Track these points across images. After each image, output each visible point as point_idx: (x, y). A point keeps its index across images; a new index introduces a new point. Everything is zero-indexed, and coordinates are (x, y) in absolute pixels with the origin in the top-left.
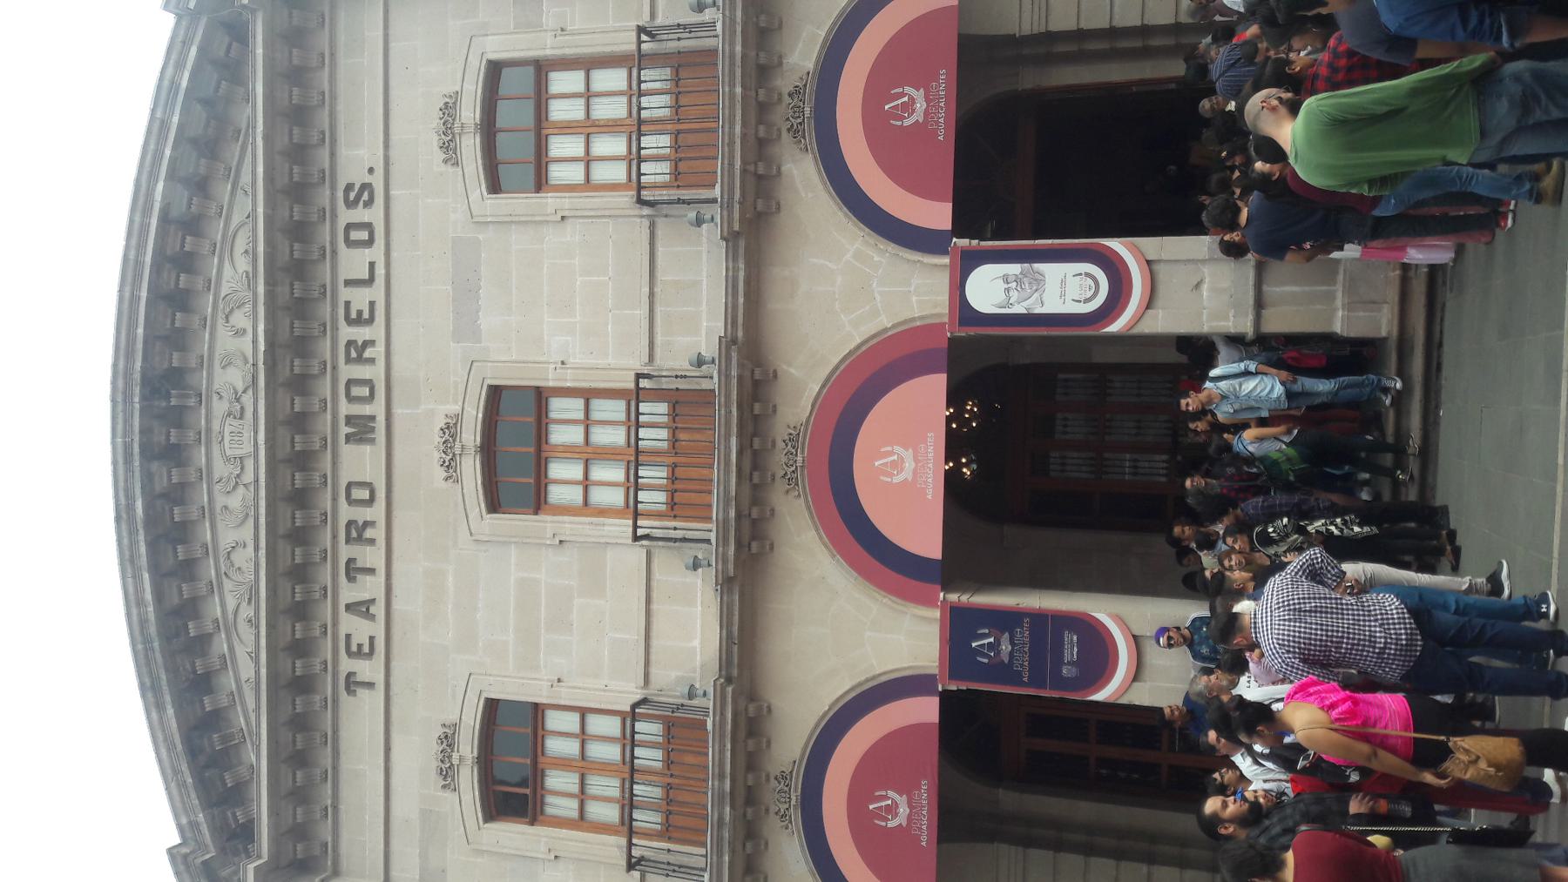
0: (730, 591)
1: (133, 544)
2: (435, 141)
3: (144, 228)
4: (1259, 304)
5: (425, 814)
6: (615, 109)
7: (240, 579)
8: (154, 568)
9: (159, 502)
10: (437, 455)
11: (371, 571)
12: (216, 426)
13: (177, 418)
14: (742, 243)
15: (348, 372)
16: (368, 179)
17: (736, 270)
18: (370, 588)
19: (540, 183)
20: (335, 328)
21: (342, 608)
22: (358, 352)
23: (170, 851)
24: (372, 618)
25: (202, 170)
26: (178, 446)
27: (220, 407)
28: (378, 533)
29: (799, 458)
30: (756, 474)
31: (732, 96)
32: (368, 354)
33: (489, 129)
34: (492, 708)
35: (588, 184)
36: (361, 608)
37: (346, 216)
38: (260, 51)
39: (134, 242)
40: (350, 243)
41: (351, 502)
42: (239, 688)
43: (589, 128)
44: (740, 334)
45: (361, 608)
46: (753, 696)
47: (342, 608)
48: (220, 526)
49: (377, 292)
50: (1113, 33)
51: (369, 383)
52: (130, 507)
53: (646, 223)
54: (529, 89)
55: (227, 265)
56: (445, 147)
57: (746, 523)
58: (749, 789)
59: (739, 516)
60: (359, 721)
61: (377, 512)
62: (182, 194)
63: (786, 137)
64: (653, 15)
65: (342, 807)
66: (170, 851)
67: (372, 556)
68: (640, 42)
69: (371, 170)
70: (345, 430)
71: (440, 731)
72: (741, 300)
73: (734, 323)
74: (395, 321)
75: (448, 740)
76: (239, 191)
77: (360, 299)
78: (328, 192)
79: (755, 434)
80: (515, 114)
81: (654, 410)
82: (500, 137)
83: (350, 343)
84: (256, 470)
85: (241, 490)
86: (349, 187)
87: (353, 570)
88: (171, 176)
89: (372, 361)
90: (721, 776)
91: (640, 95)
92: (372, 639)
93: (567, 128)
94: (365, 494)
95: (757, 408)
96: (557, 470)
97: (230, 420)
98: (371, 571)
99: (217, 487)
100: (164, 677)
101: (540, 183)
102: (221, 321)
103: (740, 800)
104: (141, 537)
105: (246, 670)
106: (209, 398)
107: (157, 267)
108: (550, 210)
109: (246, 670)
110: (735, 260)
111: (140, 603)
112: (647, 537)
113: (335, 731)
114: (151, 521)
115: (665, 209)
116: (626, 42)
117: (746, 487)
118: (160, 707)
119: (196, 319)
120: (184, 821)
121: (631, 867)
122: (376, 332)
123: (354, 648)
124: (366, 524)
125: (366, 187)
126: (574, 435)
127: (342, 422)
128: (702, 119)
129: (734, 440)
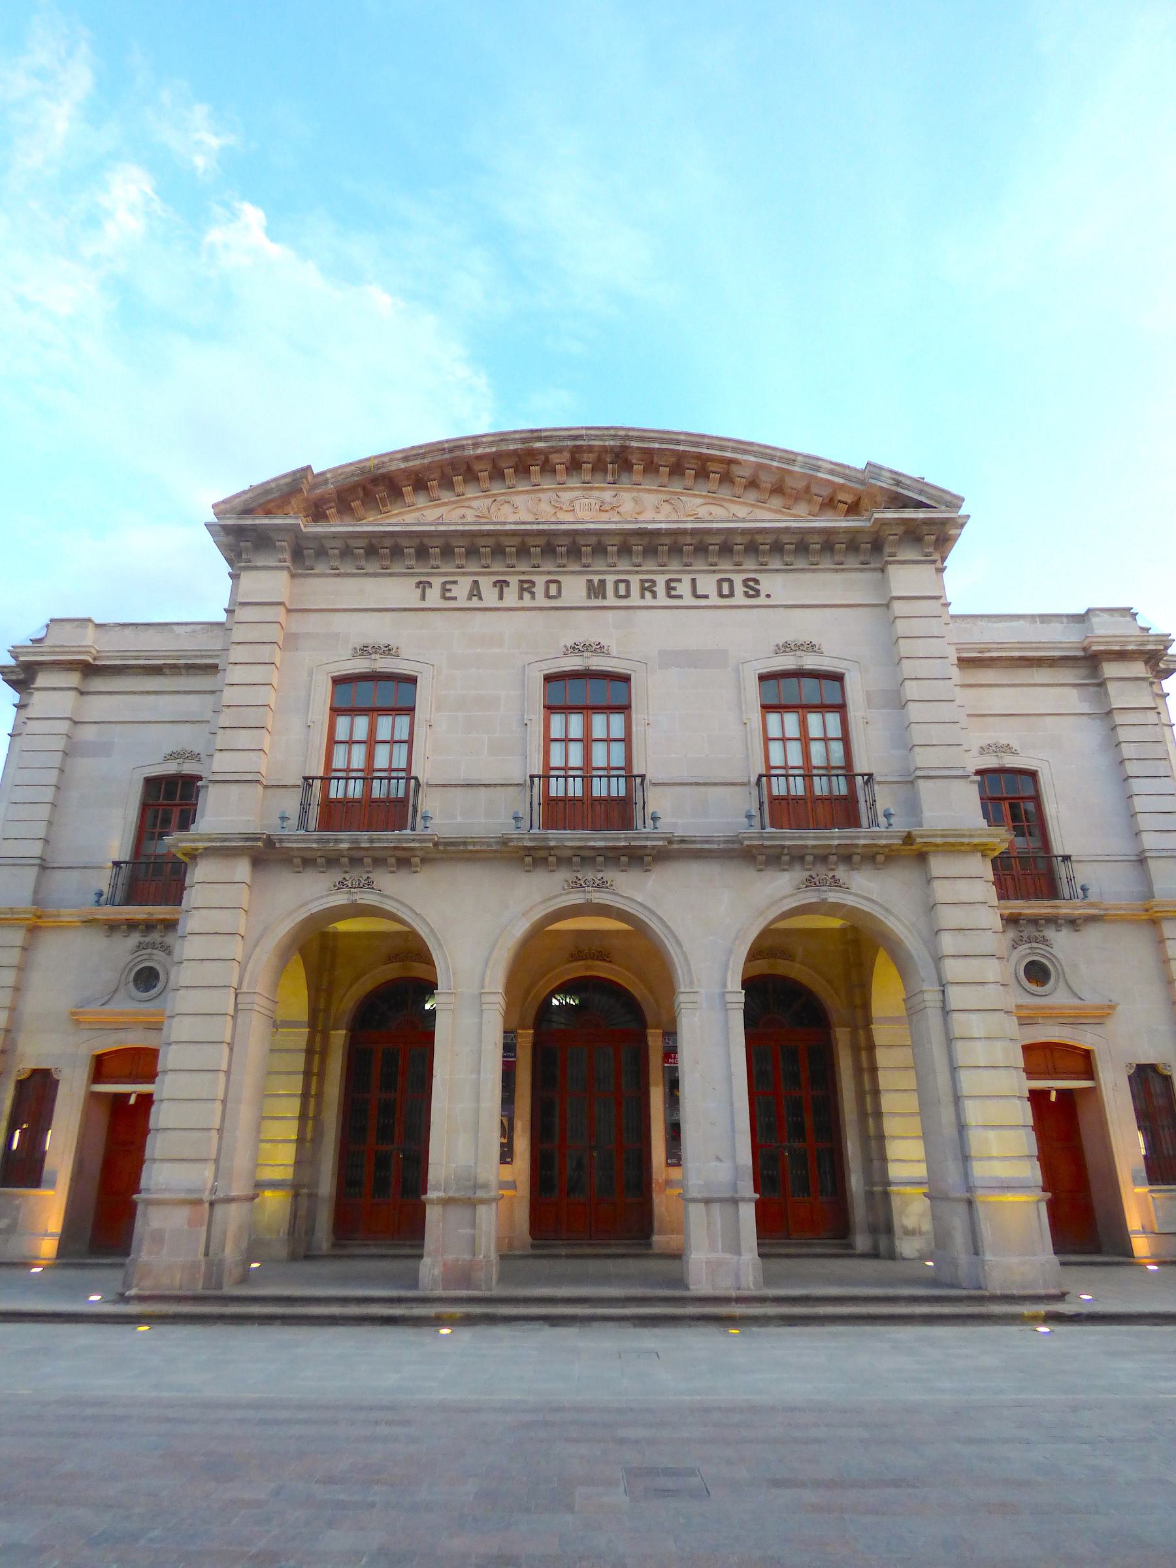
0: (498, 843)
1: (515, 441)
2: (790, 639)
3: (725, 448)
4: (708, 1201)
6: (817, 759)
7: (493, 509)
8: (498, 455)
9: (543, 457)
10: (581, 640)
11: (501, 598)
12: (596, 493)
13: (599, 467)
14: (736, 846)
15: (635, 580)
16: (763, 594)
18: (490, 596)
19: (767, 708)
20: (663, 572)
21: (475, 578)
22: (648, 588)
23: (309, 468)
24: (469, 599)
25: (763, 485)
26: (580, 468)
27: (607, 496)
29: (590, 889)
30: (578, 859)
32: (648, 594)
33: (799, 674)
34: (412, 680)
35: (767, 740)
36: (475, 591)
37: (738, 580)
38: (844, 524)
40: (720, 582)
42: (418, 509)
43: (805, 740)
44: (675, 846)
45: (475, 591)
46: (424, 860)
47: (475, 578)
49: (689, 600)
50: (876, 1092)
52: (540, 439)
53: (746, 780)
54: (827, 702)
55: (699, 501)
56: (786, 645)
57: (543, 854)
60: (396, 590)
61: (540, 600)
62: (746, 472)
64: (879, 783)
65: (338, 579)
66: (309, 468)
68: (863, 775)
69: (768, 596)
70: (596, 579)
71: (393, 645)
72: (699, 846)
73: (683, 841)
74: (668, 611)
75: (388, 651)
76: (750, 509)
77: (684, 588)
78: (753, 568)
79: (605, 858)
80: (809, 690)
81: (618, 788)
82: (795, 680)
83: (653, 582)
84: (567, 520)
86: (756, 581)
87: (501, 585)
88: (760, 466)
89: (643, 597)
90: (371, 840)
92: (455, 598)
95: (624, 859)
97: (599, 503)
98: (501, 598)
99: (552, 495)
100: (426, 461)
101: (767, 708)
102: (664, 497)
104: (519, 446)
105: (431, 514)
107: (699, 457)
109: (431, 514)
112: (532, 782)
113: (391, 575)
114: (531, 453)
115: (755, 792)
117: (570, 853)
118: (406, 459)
120: (329, 476)
121: (306, 779)
122: (662, 599)
124: (533, 594)
125: (757, 593)
126: (598, 731)
127: (602, 577)
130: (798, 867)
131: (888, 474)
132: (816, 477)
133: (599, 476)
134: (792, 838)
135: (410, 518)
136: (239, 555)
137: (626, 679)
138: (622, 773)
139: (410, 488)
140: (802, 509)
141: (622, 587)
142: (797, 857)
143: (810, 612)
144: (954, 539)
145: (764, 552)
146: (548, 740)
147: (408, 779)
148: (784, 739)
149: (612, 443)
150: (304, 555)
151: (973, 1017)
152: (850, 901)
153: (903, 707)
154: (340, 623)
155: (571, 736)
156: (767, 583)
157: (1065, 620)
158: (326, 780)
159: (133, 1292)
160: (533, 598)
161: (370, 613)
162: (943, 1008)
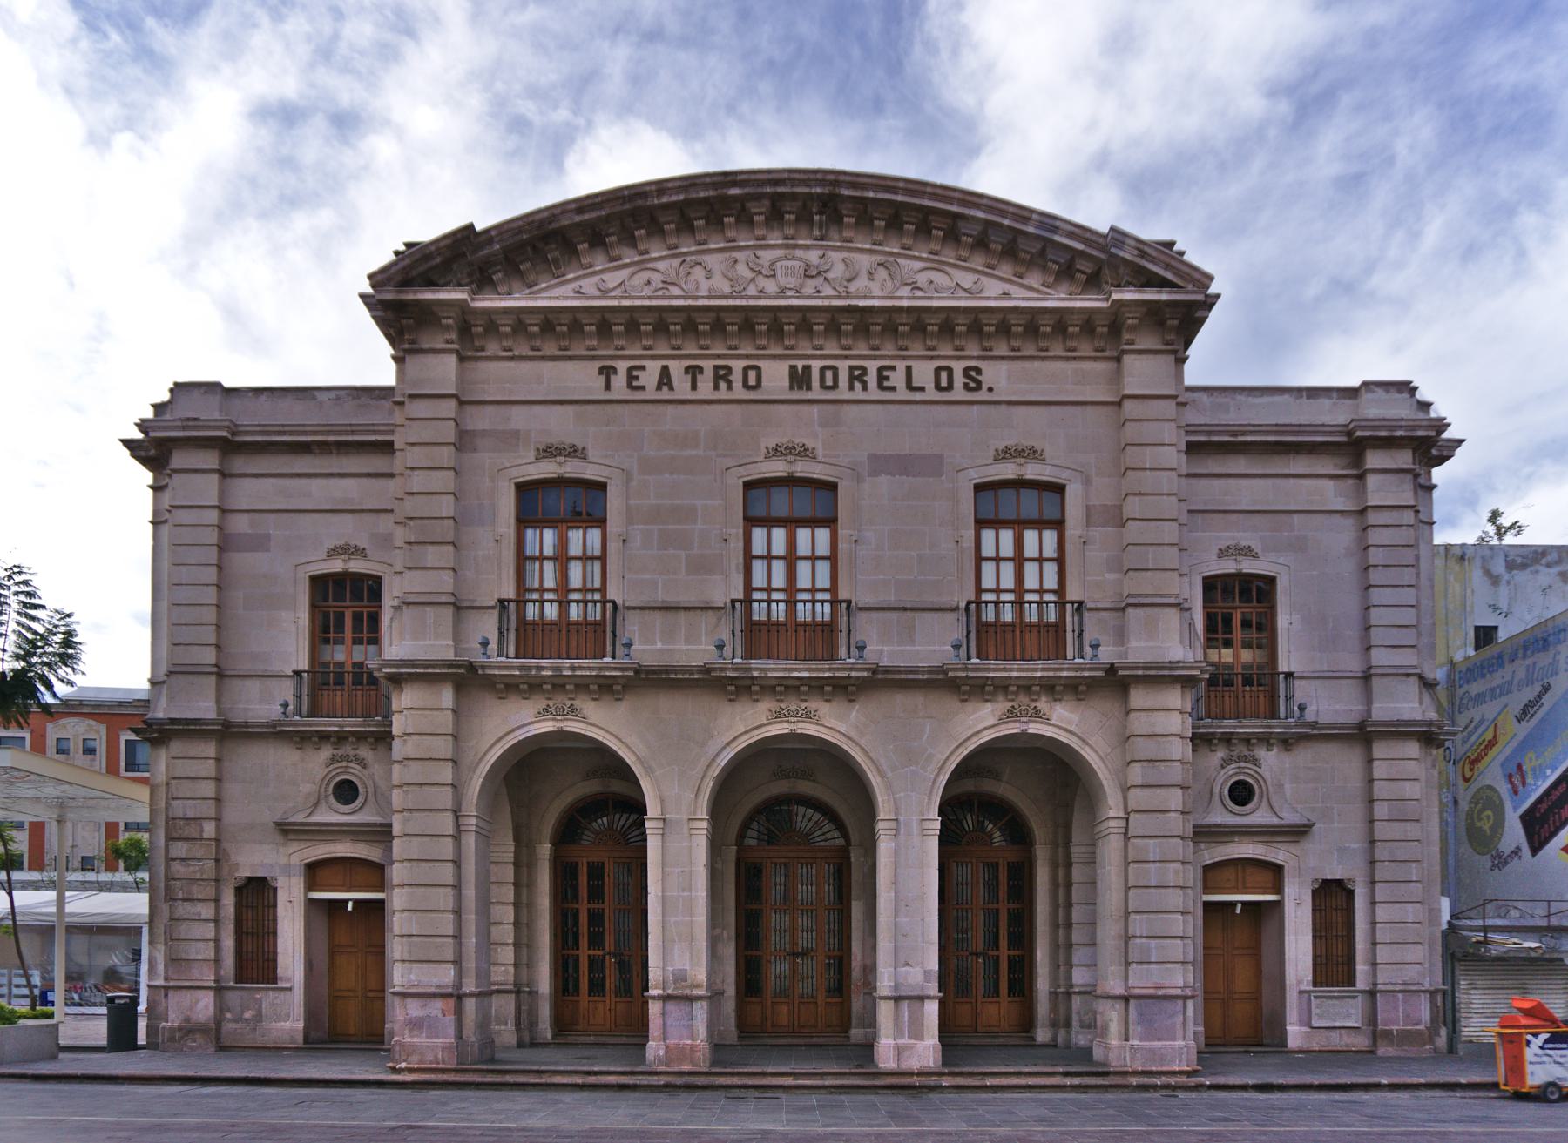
2: (1010, 443)
5: (516, 434)
10: (785, 440)
11: (694, 387)
12: (799, 253)
16: (985, 387)
17: (923, 673)
19: (981, 523)
20: (875, 358)
21: (665, 363)
25: (993, 246)
26: (782, 218)
27: (813, 256)
28: (723, 393)
31: (1036, 670)
33: (1020, 484)
39: (939, 191)
40: (938, 370)
41: (746, 369)
42: (595, 273)
45: (665, 378)
47: (665, 363)
48: (720, 256)
49: (903, 394)
51: (835, 386)
55: (919, 265)
56: (1006, 450)
57: (748, 682)
58: (563, 686)
59: (753, 678)
61: (739, 392)
63: (1009, 705)
64: (1091, 609)
67: (705, 389)
68: (1073, 603)
69: (990, 389)
70: (800, 364)
71: (580, 446)
73: (887, 672)
75: (575, 452)
76: (976, 276)
80: (1029, 504)
83: (864, 370)
85: (750, 275)
86: (978, 371)
87: (694, 372)
89: (851, 388)
91: (1039, 603)
92: (643, 388)
93: (1019, 543)
94: (752, 381)
96: (779, 534)
98: (694, 387)
101: (981, 523)
103: (556, 681)
106: (821, 247)
108: (963, 532)
109: (613, 279)
110: (930, 672)
112: (734, 607)
113: (570, 358)
116: (1073, 593)
119: (880, 237)
122: (874, 393)
123: (635, 373)
125: (979, 383)
128: (1023, 649)
129: (806, 674)
130: (1001, 698)
131: (1133, 243)
132: (1052, 241)
133: (804, 231)
134: (997, 668)
135: (589, 285)
136: (401, 332)
137: (833, 487)
138: (827, 596)
139: (586, 246)
140: (1034, 280)
141: (829, 374)
142: (1002, 687)
143: (1038, 407)
144: (1202, 320)
145: (989, 335)
146: (749, 557)
147: (604, 602)
148: (997, 559)
149: (819, 190)
150: (472, 333)
151: (1152, 841)
152: (1049, 732)
153: (1123, 525)
154: (519, 418)
155: (774, 553)
157: (1335, 395)
158: (521, 602)
159: (404, 1065)
160: (730, 388)
161: (546, 403)
162: (1125, 834)
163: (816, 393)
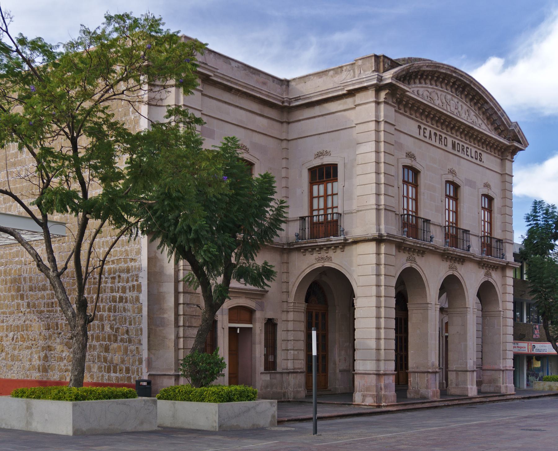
52: (455, 72)
88: (492, 108)
111: (443, 68)
156: (485, 156)
163: (456, 152)
